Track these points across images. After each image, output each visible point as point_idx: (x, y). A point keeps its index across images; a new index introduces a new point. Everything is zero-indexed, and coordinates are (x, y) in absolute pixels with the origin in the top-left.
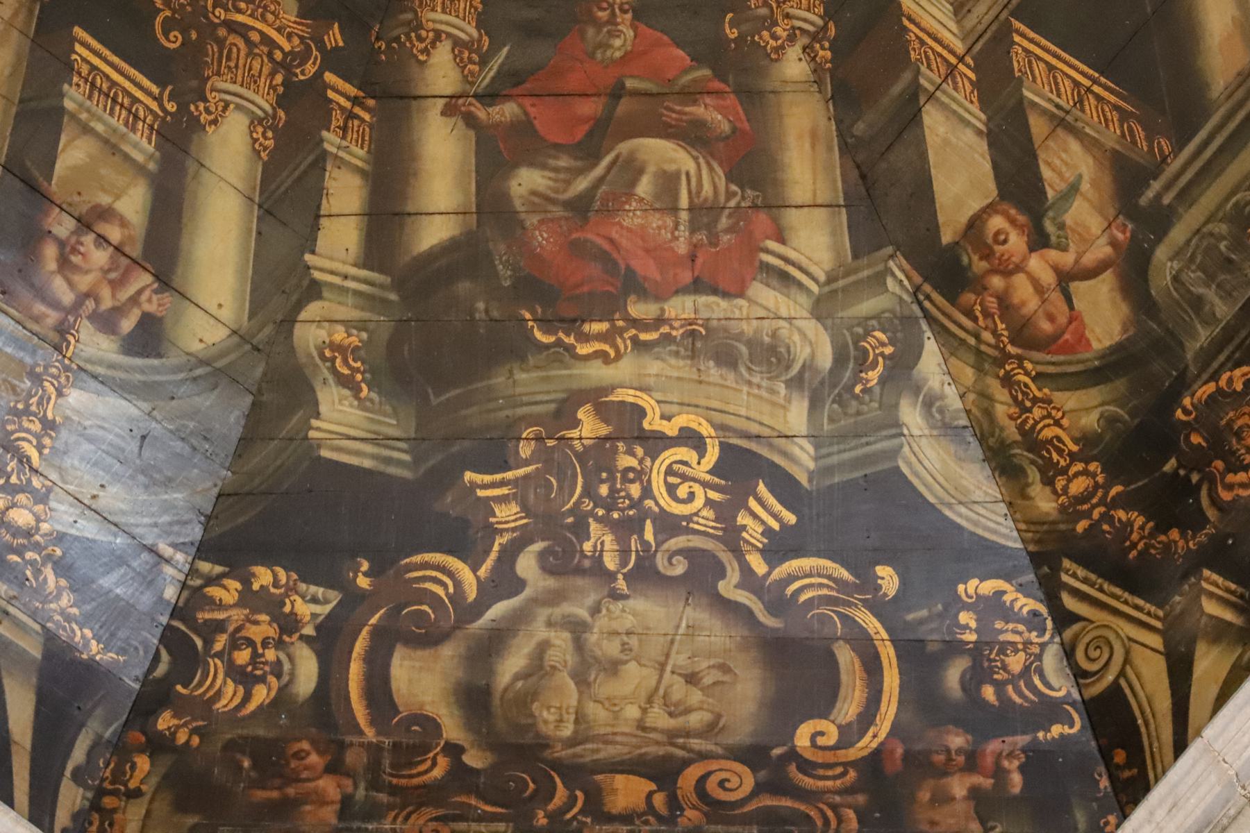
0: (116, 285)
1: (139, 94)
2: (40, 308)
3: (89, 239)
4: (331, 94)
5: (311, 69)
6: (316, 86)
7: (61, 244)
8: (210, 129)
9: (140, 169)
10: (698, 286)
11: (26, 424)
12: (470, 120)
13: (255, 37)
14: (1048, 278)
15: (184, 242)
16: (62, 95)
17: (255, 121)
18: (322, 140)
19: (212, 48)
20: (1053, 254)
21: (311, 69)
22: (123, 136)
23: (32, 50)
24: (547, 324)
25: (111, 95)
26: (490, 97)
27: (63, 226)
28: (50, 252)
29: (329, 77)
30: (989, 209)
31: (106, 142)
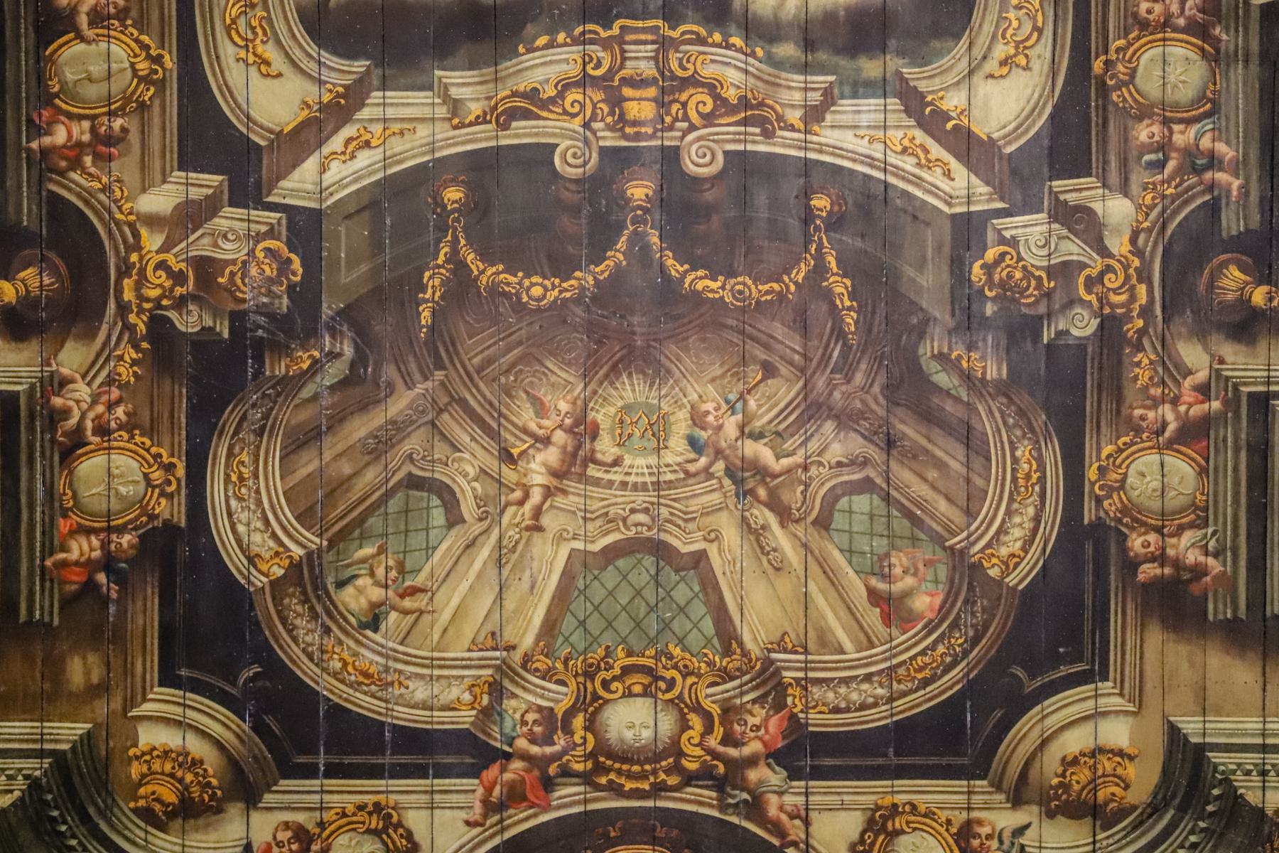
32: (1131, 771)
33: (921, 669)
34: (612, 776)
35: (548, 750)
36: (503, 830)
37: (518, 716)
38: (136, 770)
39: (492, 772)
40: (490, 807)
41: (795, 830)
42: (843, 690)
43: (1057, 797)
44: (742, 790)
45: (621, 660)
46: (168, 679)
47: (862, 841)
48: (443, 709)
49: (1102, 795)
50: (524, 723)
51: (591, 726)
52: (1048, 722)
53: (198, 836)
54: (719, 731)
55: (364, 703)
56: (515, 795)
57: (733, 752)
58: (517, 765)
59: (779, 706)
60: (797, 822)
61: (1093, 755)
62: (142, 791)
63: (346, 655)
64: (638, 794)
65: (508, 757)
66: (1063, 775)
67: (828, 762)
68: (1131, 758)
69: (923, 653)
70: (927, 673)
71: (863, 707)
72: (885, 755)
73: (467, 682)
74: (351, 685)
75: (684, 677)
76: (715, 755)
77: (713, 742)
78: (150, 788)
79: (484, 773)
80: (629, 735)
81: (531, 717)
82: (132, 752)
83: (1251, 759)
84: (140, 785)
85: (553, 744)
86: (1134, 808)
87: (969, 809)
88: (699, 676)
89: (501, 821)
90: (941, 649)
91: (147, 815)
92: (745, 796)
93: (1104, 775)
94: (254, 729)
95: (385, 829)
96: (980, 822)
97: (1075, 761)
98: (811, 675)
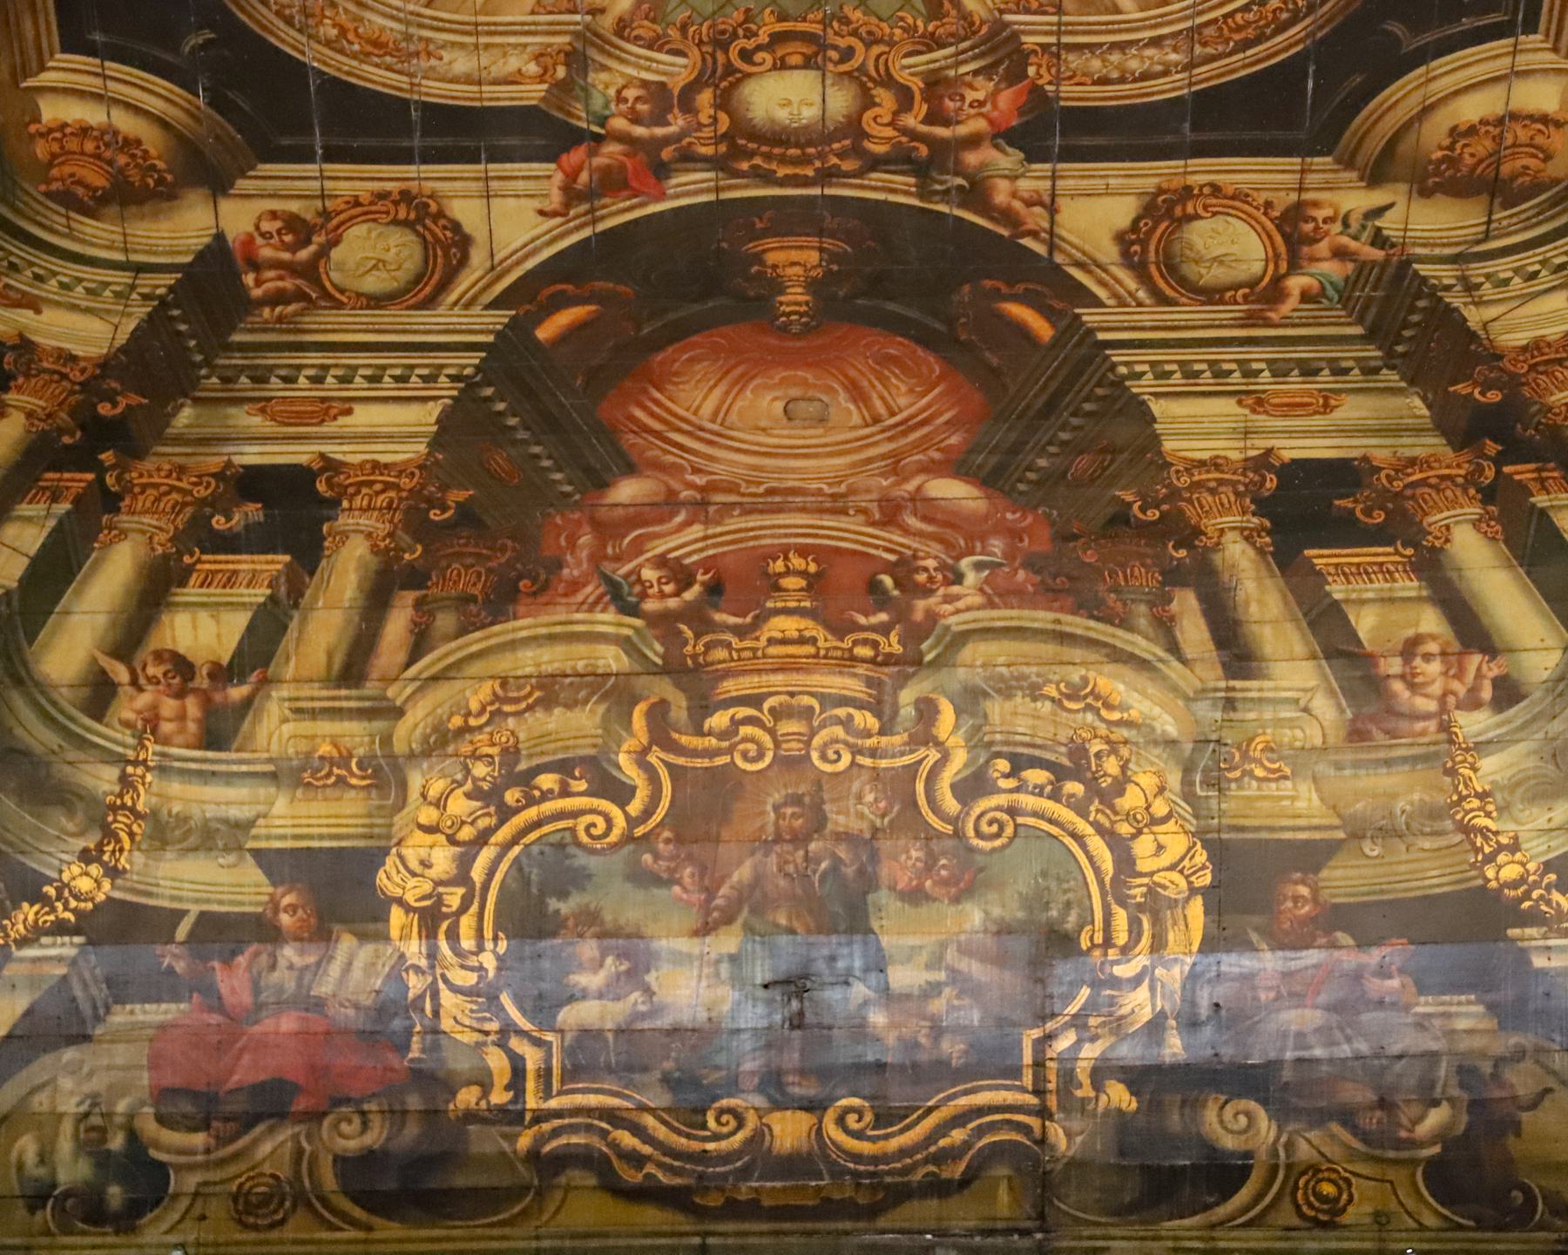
0: (1459, 676)
1: (1381, 559)
2: (1419, 726)
3: (1418, 662)
4: (1517, 477)
5: (1490, 473)
7: (1402, 677)
8: (1448, 546)
9: (1419, 599)
11: (1467, 807)
13: (1433, 481)
15: (1485, 621)
16: (1328, 595)
17: (1476, 524)
18: (1534, 505)
19: (1409, 504)
22: (1390, 589)
23: (1287, 583)
25: (1362, 571)
27: (1394, 666)
28: (1398, 686)
29: (1507, 469)
31: (1382, 600)
33: (1239, 29)
34: (758, 161)
35: (659, 131)
36: (594, 222)
37: (612, 92)
39: (576, 156)
40: (572, 195)
41: (1037, 218)
42: (1115, 57)
43: (1437, 173)
44: (957, 174)
46: (74, 42)
48: (496, 82)
49: (1506, 169)
50: (620, 99)
51: (724, 102)
52: (1434, 86)
53: (145, 224)
55: (378, 77)
56: (612, 183)
57: (941, 132)
58: (612, 149)
59: (1015, 75)
60: (1037, 210)
61: (1500, 121)
62: (55, 172)
63: (342, 18)
65: (598, 139)
66: (1451, 148)
67: (1086, 141)
68: (1558, 124)
70: (1250, 33)
71: (1145, 76)
72: (1177, 131)
74: (354, 56)
75: (868, 46)
76: (914, 135)
77: (911, 121)
78: (67, 170)
79: (564, 157)
80: (782, 115)
81: (631, 94)
82: (33, 128)
84: (50, 165)
87: (1300, 190)
89: (592, 211)
91: (67, 200)
92: (959, 181)
93: (1514, 145)
94: (210, 104)
95: (419, 220)
96: (1316, 204)
97: (1472, 130)
98: (1066, 39)
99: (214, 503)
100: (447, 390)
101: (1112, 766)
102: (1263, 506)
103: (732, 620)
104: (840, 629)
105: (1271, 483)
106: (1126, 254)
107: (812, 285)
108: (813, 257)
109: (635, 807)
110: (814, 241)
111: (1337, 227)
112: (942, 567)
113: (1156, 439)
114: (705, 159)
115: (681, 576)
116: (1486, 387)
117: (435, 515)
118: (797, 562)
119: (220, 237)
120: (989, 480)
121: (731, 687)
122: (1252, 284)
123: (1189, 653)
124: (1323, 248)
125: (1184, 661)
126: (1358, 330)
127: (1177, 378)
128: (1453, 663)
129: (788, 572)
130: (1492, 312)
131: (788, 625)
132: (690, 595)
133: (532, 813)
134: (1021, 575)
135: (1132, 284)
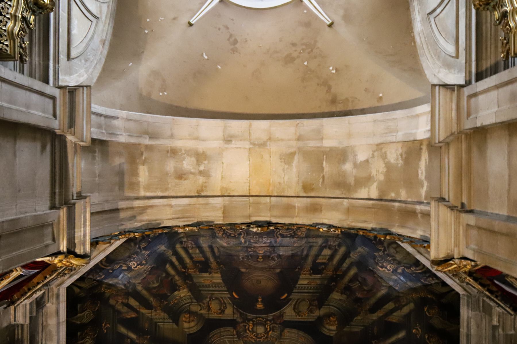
5: (186, 270)
6: (185, 270)
10: (145, 278)
12: (171, 276)
14: (119, 301)
20: (120, 302)
21: (186, 270)
24: (154, 266)
26: (172, 279)
27: (194, 246)
28: (193, 244)
29: (184, 271)
30: (128, 301)
32: (184, 319)
34: (263, 320)
35: (273, 325)
38: (336, 322)
39: (281, 322)
42: (228, 334)
45: (262, 340)
47: (225, 309)
49: (188, 315)
50: (277, 330)
52: (196, 328)
54: (247, 327)
55: (301, 333)
57: (245, 324)
58: (278, 323)
64: (260, 317)
69: (215, 339)
71: (224, 331)
73: (286, 336)
76: (247, 323)
78: (334, 319)
80: (261, 327)
81: (276, 330)
82: (337, 325)
83: (166, 321)
85: (273, 326)
86: (184, 313)
87: (208, 314)
88: (250, 337)
90: (213, 340)
95: (299, 312)
96: (207, 311)
97: (192, 321)
99: (323, 269)
100: (297, 286)
101: (224, 236)
102: (209, 267)
103: (267, 253)
104: (255, 251)
105: (209, 270)
106: (226, 305)
107: (258, 301)
108: (258, 306)
109: (279, 233)
110: (258, 308)
111: (205, 308)
112: (244, 259)
113: (222, 277)
114: (269, 321)
115: (273, 259)
116: (188, 283)
117: (299, 267)
118: (260, 260)
119: (319, 310)
120: (239, 271)
121: (268, 245)
122: (213, 300)
123: (216, 248)
124: (206, 305)
125: (217, 247)
126: (202, 292)
127: (220, 286)
128: (188, 247)
129: (261, 259)
130: (188, 294)
131: (260, 252)
132: (272, 256)
133: (291, 233)
134: (235, 258)
135: (225, 300)
